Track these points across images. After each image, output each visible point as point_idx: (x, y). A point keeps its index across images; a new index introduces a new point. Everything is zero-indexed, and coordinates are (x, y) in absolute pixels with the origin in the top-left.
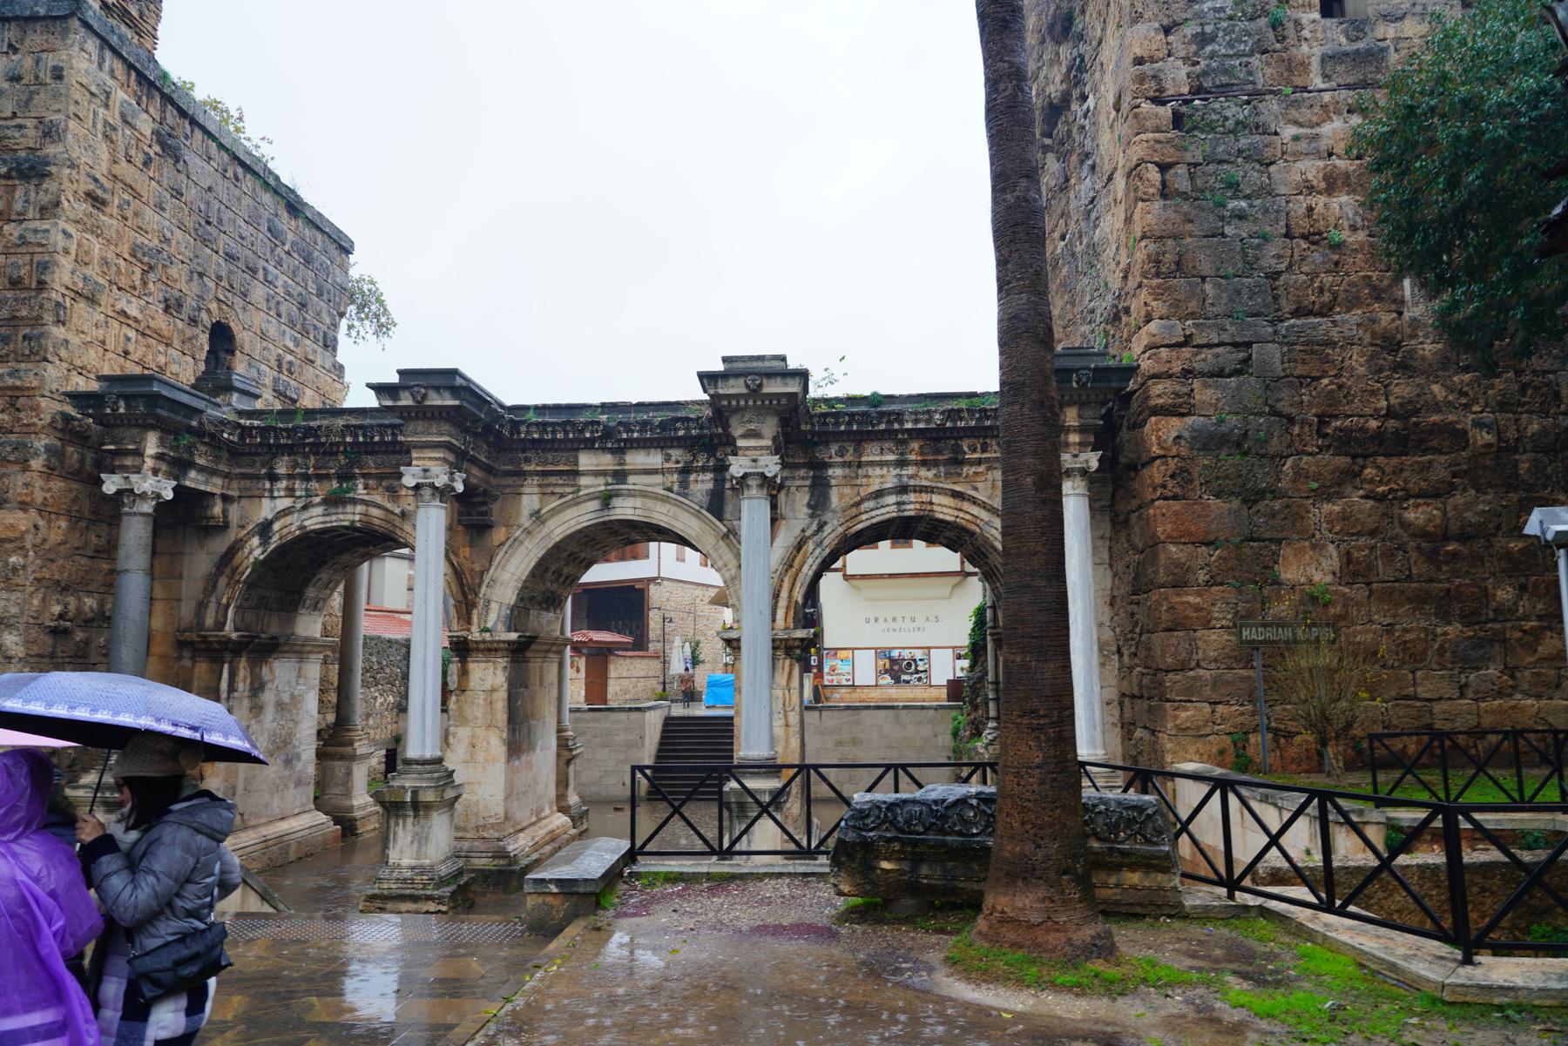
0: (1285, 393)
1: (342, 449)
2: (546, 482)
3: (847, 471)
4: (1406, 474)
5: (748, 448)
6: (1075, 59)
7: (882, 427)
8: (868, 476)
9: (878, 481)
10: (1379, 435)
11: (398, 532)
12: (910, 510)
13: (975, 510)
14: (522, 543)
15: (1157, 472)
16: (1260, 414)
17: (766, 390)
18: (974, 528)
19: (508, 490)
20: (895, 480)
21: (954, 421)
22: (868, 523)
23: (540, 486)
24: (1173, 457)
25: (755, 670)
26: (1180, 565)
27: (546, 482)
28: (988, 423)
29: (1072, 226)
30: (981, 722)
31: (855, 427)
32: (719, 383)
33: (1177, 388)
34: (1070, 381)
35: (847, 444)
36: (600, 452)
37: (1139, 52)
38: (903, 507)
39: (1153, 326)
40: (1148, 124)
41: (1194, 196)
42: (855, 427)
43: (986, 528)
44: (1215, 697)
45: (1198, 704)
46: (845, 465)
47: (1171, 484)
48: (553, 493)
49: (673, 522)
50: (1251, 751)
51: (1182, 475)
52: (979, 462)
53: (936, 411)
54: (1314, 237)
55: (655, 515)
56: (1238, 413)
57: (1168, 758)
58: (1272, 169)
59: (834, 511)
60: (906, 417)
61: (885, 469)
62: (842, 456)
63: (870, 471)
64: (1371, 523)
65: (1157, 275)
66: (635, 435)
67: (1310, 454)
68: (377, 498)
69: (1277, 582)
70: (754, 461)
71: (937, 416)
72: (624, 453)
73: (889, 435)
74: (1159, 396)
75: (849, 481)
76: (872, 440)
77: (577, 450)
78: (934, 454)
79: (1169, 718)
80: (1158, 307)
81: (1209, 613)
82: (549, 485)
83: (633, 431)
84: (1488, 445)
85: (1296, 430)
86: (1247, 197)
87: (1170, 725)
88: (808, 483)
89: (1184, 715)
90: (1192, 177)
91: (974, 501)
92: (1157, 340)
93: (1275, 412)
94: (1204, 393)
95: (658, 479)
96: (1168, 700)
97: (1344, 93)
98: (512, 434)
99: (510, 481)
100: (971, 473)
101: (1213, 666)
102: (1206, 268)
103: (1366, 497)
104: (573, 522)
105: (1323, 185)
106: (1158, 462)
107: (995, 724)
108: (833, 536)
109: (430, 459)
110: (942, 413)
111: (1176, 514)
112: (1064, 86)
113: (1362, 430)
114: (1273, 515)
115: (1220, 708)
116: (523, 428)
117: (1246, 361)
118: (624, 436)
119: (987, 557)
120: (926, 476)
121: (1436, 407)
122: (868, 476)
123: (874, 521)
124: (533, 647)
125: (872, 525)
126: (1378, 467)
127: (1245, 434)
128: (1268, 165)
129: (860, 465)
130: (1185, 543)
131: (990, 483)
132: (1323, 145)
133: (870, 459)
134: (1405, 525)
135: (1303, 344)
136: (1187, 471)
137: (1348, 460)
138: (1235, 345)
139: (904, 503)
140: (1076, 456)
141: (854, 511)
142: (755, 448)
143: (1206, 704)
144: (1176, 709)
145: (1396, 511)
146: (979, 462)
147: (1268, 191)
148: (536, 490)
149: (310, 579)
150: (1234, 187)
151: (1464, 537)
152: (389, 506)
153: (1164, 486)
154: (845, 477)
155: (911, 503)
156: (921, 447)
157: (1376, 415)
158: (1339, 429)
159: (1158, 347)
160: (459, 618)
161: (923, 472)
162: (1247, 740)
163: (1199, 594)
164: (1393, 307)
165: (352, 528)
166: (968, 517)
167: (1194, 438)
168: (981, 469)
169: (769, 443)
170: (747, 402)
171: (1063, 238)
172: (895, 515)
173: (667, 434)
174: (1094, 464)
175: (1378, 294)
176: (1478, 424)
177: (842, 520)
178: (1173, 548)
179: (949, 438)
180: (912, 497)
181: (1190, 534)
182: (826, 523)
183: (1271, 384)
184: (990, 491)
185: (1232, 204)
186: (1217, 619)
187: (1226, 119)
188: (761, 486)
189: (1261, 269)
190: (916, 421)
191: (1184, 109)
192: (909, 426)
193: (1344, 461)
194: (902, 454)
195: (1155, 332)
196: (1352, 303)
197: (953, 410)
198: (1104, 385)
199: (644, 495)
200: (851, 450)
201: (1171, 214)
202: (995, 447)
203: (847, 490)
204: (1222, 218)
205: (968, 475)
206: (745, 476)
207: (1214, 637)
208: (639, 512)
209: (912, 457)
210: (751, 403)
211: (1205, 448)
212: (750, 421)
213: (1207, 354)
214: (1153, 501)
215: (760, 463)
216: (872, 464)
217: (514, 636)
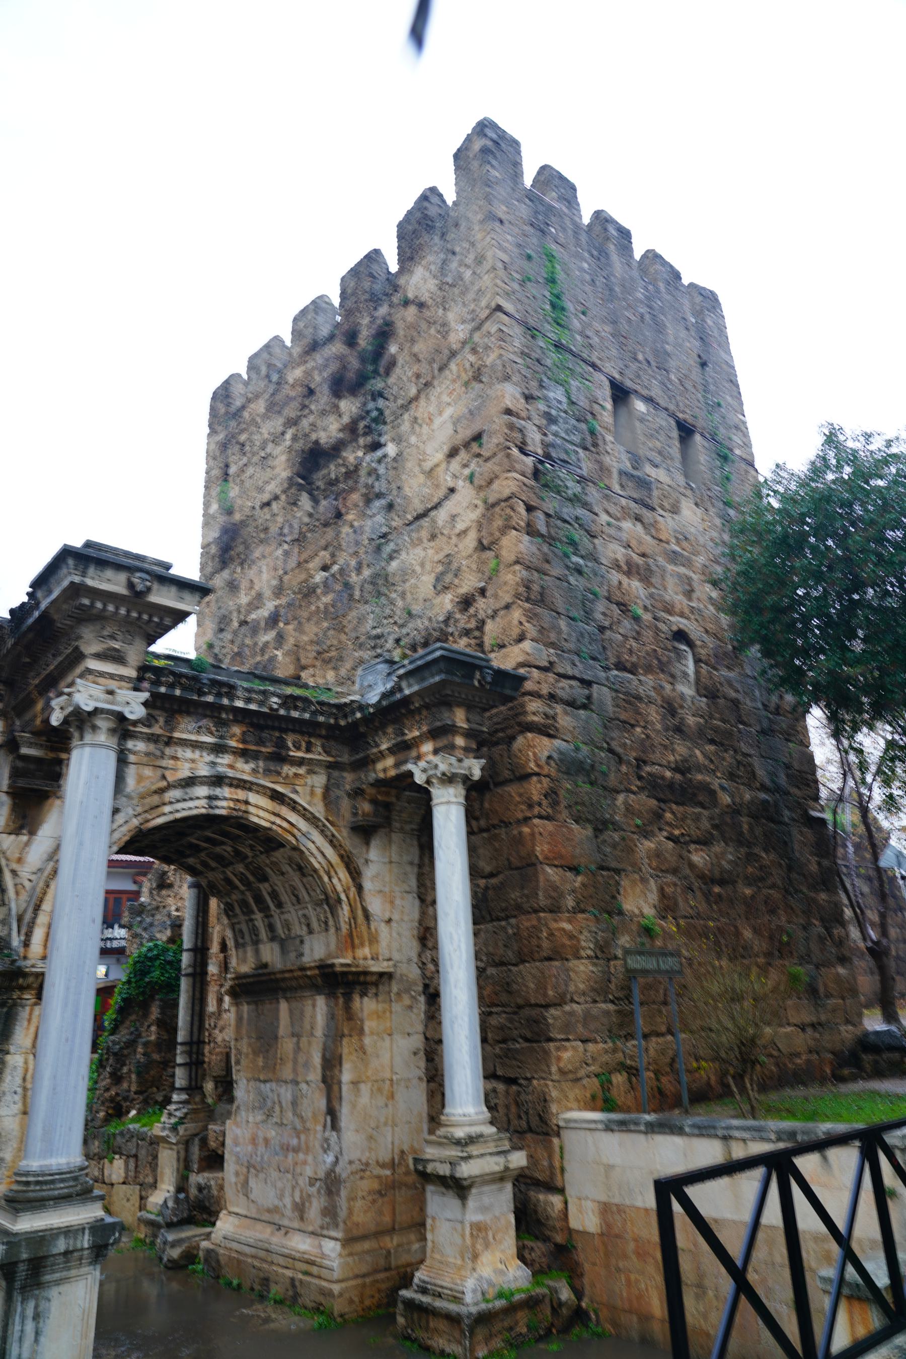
0: (615, 734)
3: (152, 747)
4: (689, 822)
5: (102, 674)
6: (368, 412)
7: (210, 699)
8: (175, 758)
9: (187, 765)
10: (671, 785)
12: (222, 808)
13: (293, 818)
15: (535, 789)
16: (601, 748)
17: (154, 598)
18: (290, 838)
20: (207, 768)
21: (288, 709)
22: (170, 818)
25: (76, 1015)
26: (555, 888)
28: (321, 719)
29: (343, 558)
30: (126, 1099)
31: (178, 692)
32: (91, 570)
33: (547, 710)
34: (472, 678)
37: (511, 406)
39: (527, 645)
40: (517, 466)
41: (549, 539)
43: (303, 840)
44: (586, 1034)
45: (574, 1043)
46: (152, 739)
50: (614, 1092)
51: (551, 794)
52: (300, 762)
53: (274, 694)
54: (623, 607)
56: (586, 744)
57: (554, 1108)
58: (596, 541)
59: (129, 797)
60: (239, 693)
61: (198, 753)
62: (149, 726)
63: (180, 752)
64: (673, 860)
65: (528, 600)
67: (634, 793)
69: (621, 913)
70: (111, 693)
71: (275, 699)
73: (213, 712)
74: (534, 714)
75: (151, 760)
76: (189, 713)
78: (257, 744)
79: (554, 1061)
80: (531, 629)
81: (578, 940)
84: (728, 806)
85: (624, 769)
86: (582, 557)
87: (554, 1069)
89: (566, 1055)
90: (548, 525)
91: (294, 806)
92: (531, 659)
93: (611, 751)
94: (565, 720)
96: (550, 1040)
97: (632, 505)
100: (291, 773)
101: (581, 1000)
102: (561, 606)
103: (668, 838)
105: (625, 568)
106: (535, 779)
107: (184, 1097)
108: (124, 829)
110: (278, 696)
111: (551, 834)
112: (341, 435)
113: (663, 778)
114: (614, 846)
115: (591, 1046)
117: (589, 698)
119: (264, 878)
120: (244, 769)
121: (699, 768)
122: (175, 758)
123: (178, 815)
125: (176, 821)
126: (673, 813)
127: (592, 766)
128: (594, 537)
129: (169, 742)
130: (556, 866)
131: (308, 789)
132: (624, 536)
133: (184, 736)
134: (692, 865)
135: (625, 694)
136: (555, 793)
137: (655, 802)
138: (582, 681)
139: (216, 798)
140: (460, 760)
141: (156, 799)
142: (112, 676)
143: (579, 1043)
144: (558, 1049)
145: (685, 853)
146: (300, 762)
147: (592, 557)
150: (573, 543)
151: (722, 882)
153: (540, 805)
154: (147, 754)
155: (225, 799)
156: (244, 733)
157: (669, 768)
158: (649, 774)
159: (530, 666)
161: (240, 764)
162: (610, 1082)
163: (570, 921)
164: (671, 680)
166: (285, 824)
167: (561, 760)
168: (302, 771)
169: (133, 674)
170: (117, 608)
171: (325, 568)
172: (203, 811)
174: (477, 774)
175: (663, 667)
176: (723, 788)
177: (139, 809)
178: (549, 870)
179: (273, 728)
180: (226, 792)
181: (561, 857)
183: (609, 722)
184: (308, 798)
185: (575, 559)
186: (584, 948)
187: (567, 488)
188: (112, 731)
189: (594, 620)
190: (248, 700)
191: (540, 467)
192: (239, 704)
193: (653, 803)
194: (221, 737)
195: (530, 651)
196: (649, 669)
197: (291, 696)
198: (499, 689)
200: (161, 720)
201: (534, 549)
202: (320, 749)
203: (148, 772)
204: (568, 567)
206: (96, 711)
207: (582, 968)
209: (233, 743)
211: (567, 773)
212: (112, 637)
213: (564, 683)
214: (527, 819)
215: (119, 698)
216: (184, 743)
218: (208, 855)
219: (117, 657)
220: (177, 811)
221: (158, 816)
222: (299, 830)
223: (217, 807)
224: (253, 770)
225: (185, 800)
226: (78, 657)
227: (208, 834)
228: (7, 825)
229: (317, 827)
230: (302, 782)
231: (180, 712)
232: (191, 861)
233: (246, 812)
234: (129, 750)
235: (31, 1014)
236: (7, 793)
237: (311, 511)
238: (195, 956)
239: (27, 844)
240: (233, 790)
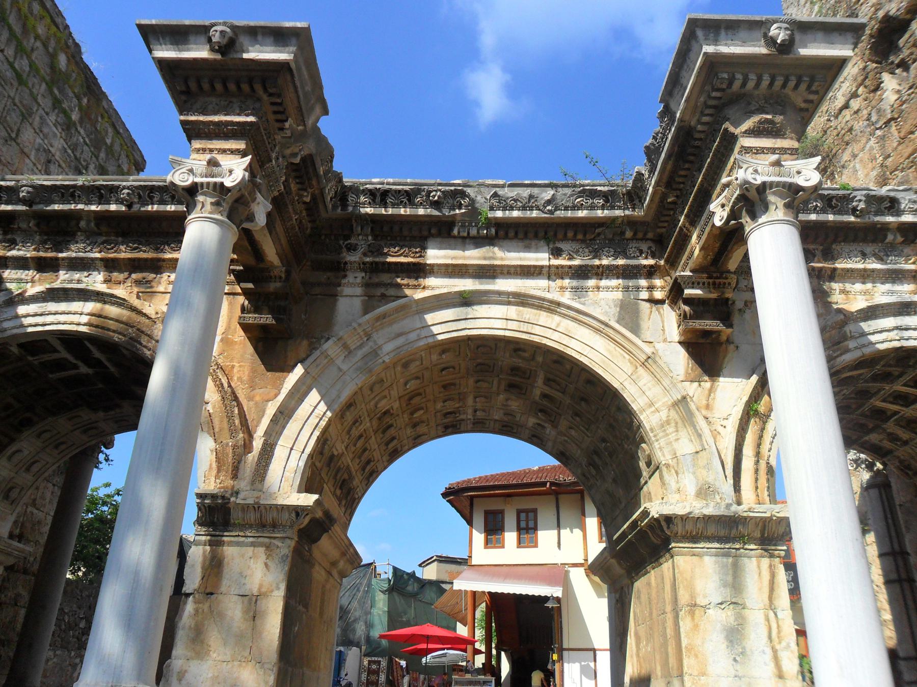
1: (83, 224)
2: (376, 280)
11: (144, 340)
19: (317, 290)
23: (367, 285)
27: (376, 280)
36: (460, 240)
48: (383, 296)
49: (565, 340)
55: (537, 330)
68: (120, 292)
95: (543, 283)
98: (335, 207)
99: (323, 277)
109: (223, 151)
116: (351, 198)
118: (499, 214)
142: (773, 151)
148: (359, 291)
149: (6, 446)
152: (136, 303)
160: (219, 470)
165: (69, 339)
172: (897, 344)
173: (560, 214)
199: (521, 300)
208: (513, 325)
210: (766, 82)
217: (309, 499)
218: (898, 423)
226: (730, 140)
227: (899, 387)
228: (687, 373)
231: (835, 241)
232: (874, 438)
235: (759, 567)
236: (680, 343)
237: (898, 87)
238: (895, 560)
239: (711, 390)
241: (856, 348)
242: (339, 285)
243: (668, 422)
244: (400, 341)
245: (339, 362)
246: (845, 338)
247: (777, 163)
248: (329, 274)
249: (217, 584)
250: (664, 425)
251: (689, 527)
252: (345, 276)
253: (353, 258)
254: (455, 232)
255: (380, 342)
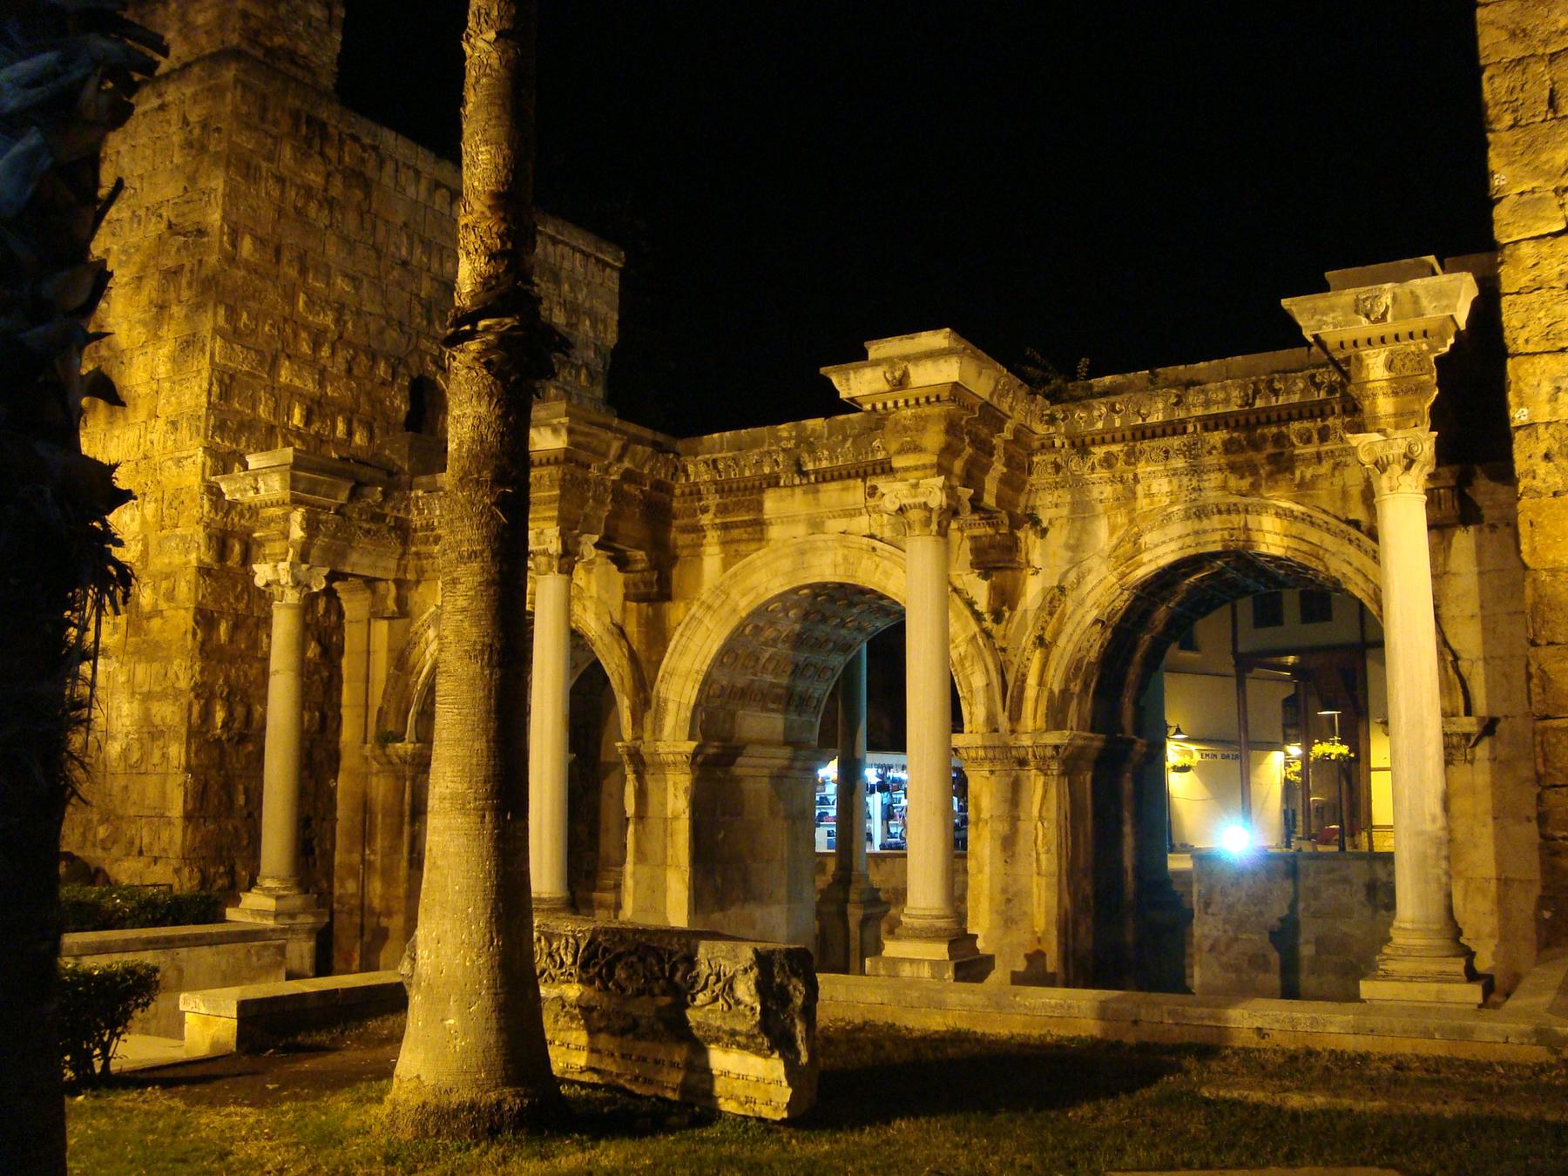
3: (1119, 487)
5: (906, 469)
8: (1149, 495)
14: (701, 621)
18: (1314, 564)
23: (724, 543)
24: (1548, 424)
35: (1115, 448)
36: (788, 491)
38: (1204, 538)
42: (1118, 423)
47: (1542, 468)
52: (1319, 458)
66: (825, 464)
72: (817, 491)
77: (761, 490)
82: (733, 541)
83: (820, 460)
88: (1065, 511)
104: (762, 590)
108: (1100, 590)
109: (545, 519)
124: (740, 760)
139: (1205, 532)
142: (916, 468)
161: (1234, 482)
168: (1326, 467)
179: (1269, 422)
180: (1216, 521)
182: (1090, 571)
192: (1199, 412)
205: (1302, 478)
219: (917, 449)
220: (1158, 557)
221: (1139, 567)
222: (1326, 550)
223: (1206, 543)
224: (1252, 484)
225: (1164, 542)
229: (1350, 541)
230: (1326, 484)
233: (1248, 540)
234: (1096, 500)
240: (1225, 516)
241: (1150, 561)
242: (702, 545)
243: (965, 657)
244: (750, 597)
245: (706, 621)
246: (1138, 551)
247: (916, 486)
248: (693, 536)
249: (646, 811)
250: (962, 659)
251: (972, 753)
252: (705, 537)
253: (706, 519)
254: (782, 483)
255: (738, 598)
